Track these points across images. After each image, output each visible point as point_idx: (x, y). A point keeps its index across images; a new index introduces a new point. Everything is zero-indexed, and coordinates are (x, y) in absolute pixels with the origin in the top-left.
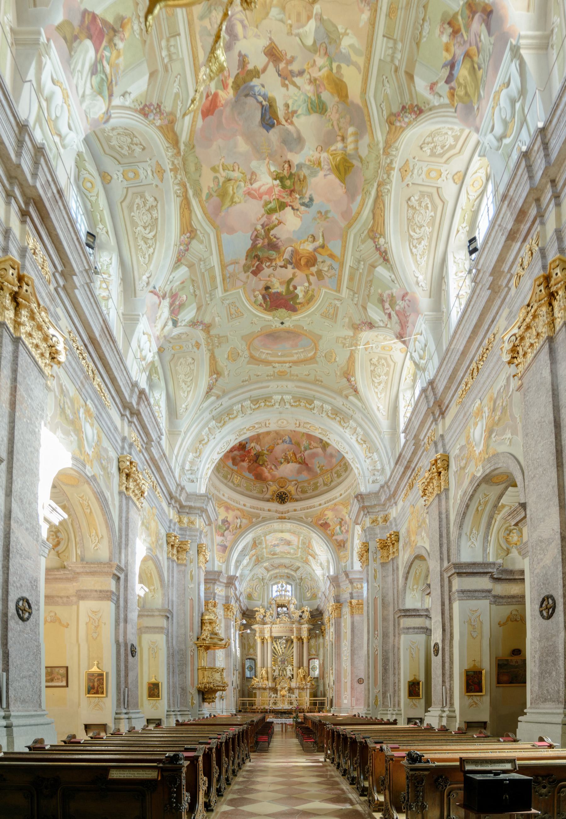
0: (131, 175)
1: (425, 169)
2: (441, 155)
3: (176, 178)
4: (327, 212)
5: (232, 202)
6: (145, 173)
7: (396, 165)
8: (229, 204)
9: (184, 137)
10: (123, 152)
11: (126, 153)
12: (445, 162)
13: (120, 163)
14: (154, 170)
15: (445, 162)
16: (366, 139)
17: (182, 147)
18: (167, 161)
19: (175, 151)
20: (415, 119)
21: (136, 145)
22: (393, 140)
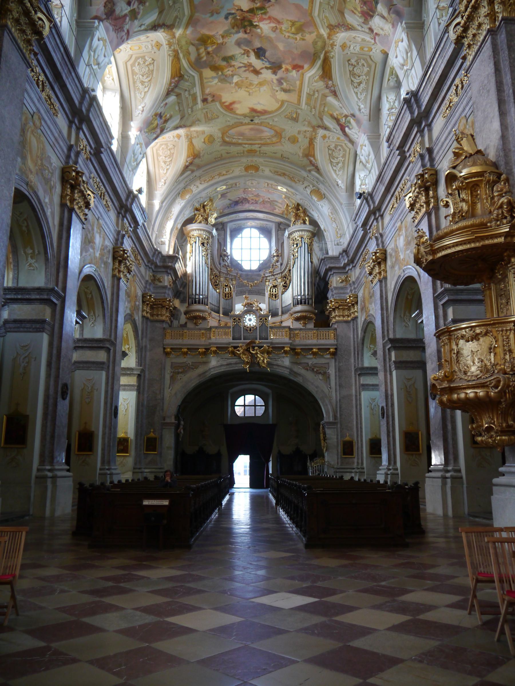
0: (366, 49)
1: (144, 49)
2: (137, 58)
3: (333, 42)
4: (212, 15)
5: (293, 24)
6: (355, 48)
7: (165, 47)
8: (296, 23)
9: (319, 63)
10: (363, 62)
11: (362, 60)
12: (132, 56)
13: (370, 56)
14: (348, 48)
15: (132, 56)
16: (193, 57)
17: (322, 56)
18: (336, 51)
19: (328, 54)
20: (168, 89)
21: (352, 65)
22: (174, 62)
